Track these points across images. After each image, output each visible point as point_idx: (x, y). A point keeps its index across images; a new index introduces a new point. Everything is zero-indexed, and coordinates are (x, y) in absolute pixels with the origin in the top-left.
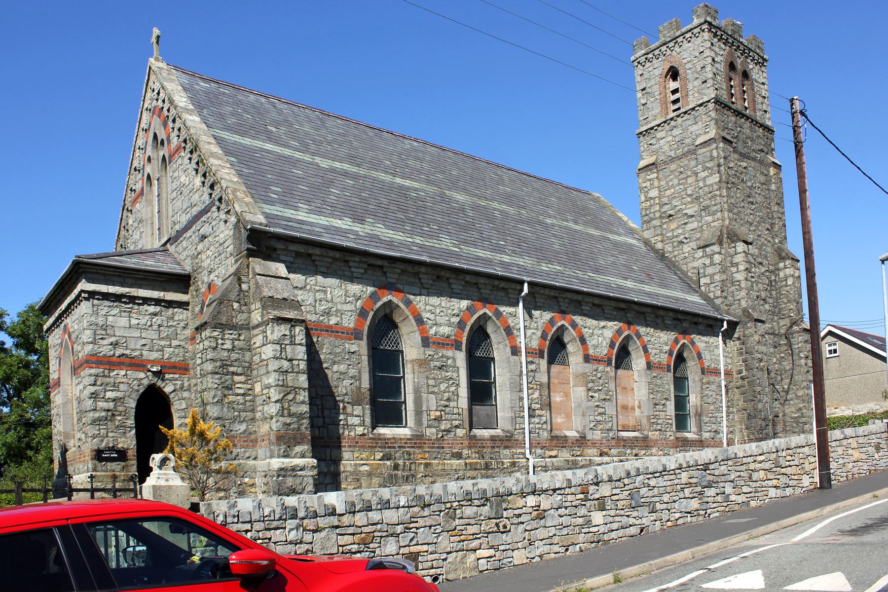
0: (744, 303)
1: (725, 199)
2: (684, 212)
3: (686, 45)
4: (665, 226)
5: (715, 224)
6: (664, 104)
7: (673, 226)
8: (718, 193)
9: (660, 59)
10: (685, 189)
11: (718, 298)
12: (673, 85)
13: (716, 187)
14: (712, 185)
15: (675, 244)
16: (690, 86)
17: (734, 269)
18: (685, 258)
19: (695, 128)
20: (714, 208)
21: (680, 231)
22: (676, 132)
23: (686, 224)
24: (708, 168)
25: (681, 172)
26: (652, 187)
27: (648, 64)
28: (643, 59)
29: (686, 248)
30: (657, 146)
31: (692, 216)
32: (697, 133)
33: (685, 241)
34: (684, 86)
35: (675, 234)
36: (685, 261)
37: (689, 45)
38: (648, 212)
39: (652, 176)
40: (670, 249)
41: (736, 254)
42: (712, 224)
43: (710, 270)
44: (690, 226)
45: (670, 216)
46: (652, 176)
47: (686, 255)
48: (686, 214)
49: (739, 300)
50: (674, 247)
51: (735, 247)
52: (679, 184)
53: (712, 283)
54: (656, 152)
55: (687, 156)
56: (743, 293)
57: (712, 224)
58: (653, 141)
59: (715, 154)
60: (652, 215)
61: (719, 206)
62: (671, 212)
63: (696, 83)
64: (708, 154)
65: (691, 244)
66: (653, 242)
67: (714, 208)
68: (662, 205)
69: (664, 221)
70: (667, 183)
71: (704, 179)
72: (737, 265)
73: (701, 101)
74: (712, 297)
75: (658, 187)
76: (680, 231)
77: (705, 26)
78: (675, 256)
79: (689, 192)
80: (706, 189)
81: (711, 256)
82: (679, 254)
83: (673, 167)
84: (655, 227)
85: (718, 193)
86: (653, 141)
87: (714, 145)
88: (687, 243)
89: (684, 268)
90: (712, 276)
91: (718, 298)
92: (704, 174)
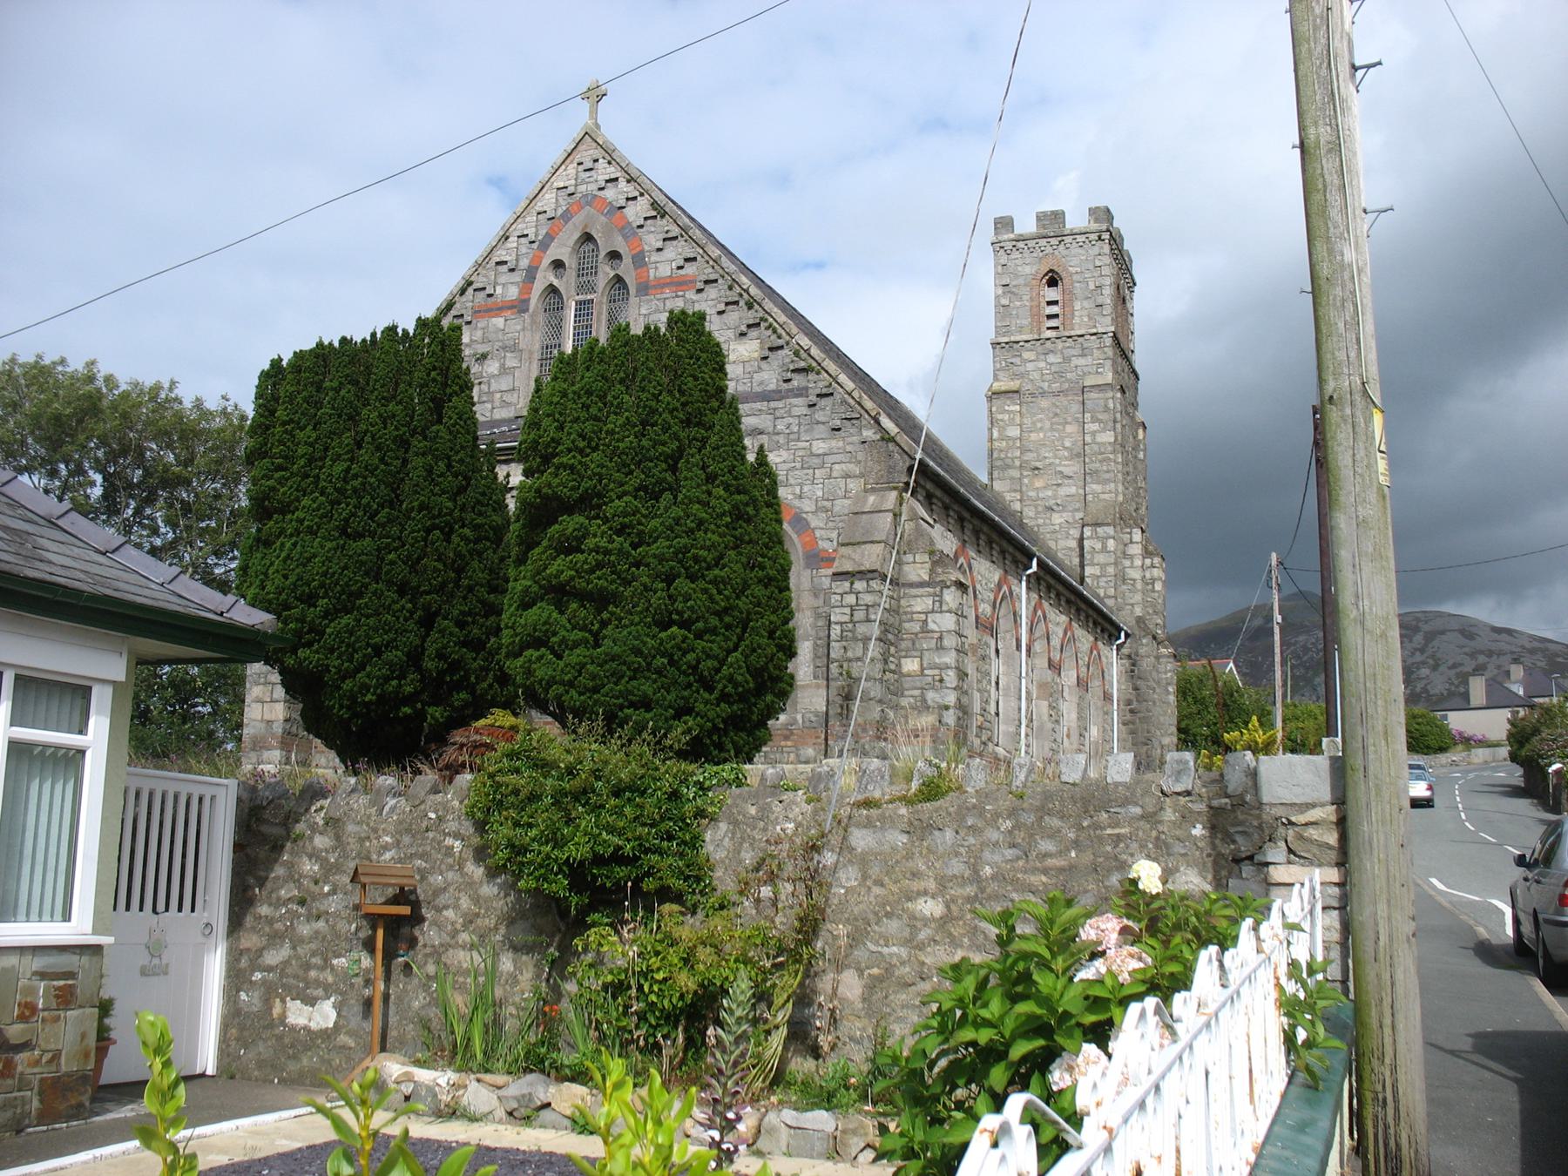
0: (1138, 611)
1: (1120, 467)
2: (1059, 469)
3: (1075, 250)
4: (1026, 481)
5: (1106, 496)
6: (1035, 314)
7: (1039, 483)
8: (1111, 456)
9: (1035, 255)
10: (1061, 439)
11: (1109, 597)
12: (1052, 294)
13: (1110, 448)
14: (1103, 444)
15: (1040, 509)
16: (1077, 305)
17: (1127, 563)
18: (1055, 532)
19: (1081, 361)
20: (1107, 476)
21: (1050, 493)
22: (1051, 358)
23: (1058, 485)
24: (1100, 421)
25: (1056, 414)
26: (1012, 422)
27: (1016, 254)
28: (1009, 246)
29: (1057, 519)
30: (1022, 369)
31: (1070, 477)
32: (1085, 369)
33: (1055, 507)
34: (1070, 297)
35: (1041, 495)
36: (1054, 536)
37: (1080, 251)
38: (1003, 456)
39: (1012, 408)
40: (1031, 514)
41: (1131, 542)
42: (1102, 496)
43: (1101, 558)
44: (1063, 491)
45: (1037, 469)
46: (1012, 408)
47: (1057, 527)
48: (1061, 472)
49: (1132, 605)
50: (1038, 513)
51: (1130, 533)
52: (1052, 429)
53: (1102, 576)
54: (1021, 376)
55: (1067, 395)
56: (1138, 597)
57: (1102, 496)
58: (1017, 361)
59: (1111, 405)
60: (1009, 461)
61: (1112, 475)
62: (1038, 464)
63: (1086, 304)
64: (1102, 402)
65: (1064, 515)
66: (1008, 498)
67: (1107, 476)
68: (1024, 450)
69: (1025, 473)
70: (1034, 423)
71: (1094, 433)
72: (1131, 557)
73: (1094, 331)
74: (1102, 594)
75: (1020, 425)
76: (1050, 493)
77: (1106, 236)
78: (1038, 526)
79: (1067, 444)
80: (1096, 448)
81: (1104, 540)
82: (1045, 524)
83: (1044, 403)
84: (1012, 478)
85: (1111, 456)
86: (1017, 361)
87: (1110, 394)
88: (1059, 512)
89: (1052, 544)
90: (1103, 566)
91: (1109, 597)
92: (1095, 427)
